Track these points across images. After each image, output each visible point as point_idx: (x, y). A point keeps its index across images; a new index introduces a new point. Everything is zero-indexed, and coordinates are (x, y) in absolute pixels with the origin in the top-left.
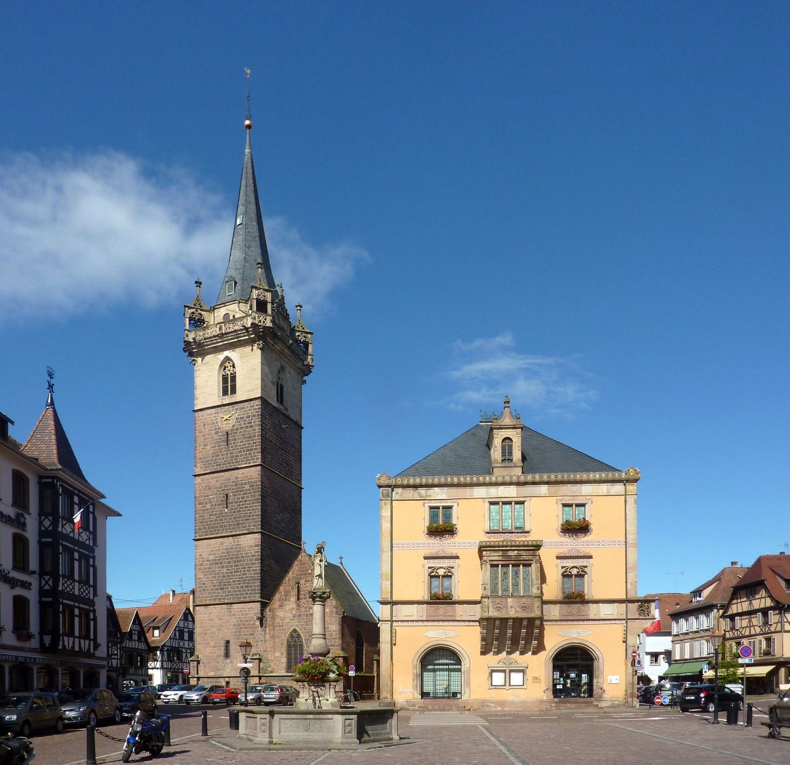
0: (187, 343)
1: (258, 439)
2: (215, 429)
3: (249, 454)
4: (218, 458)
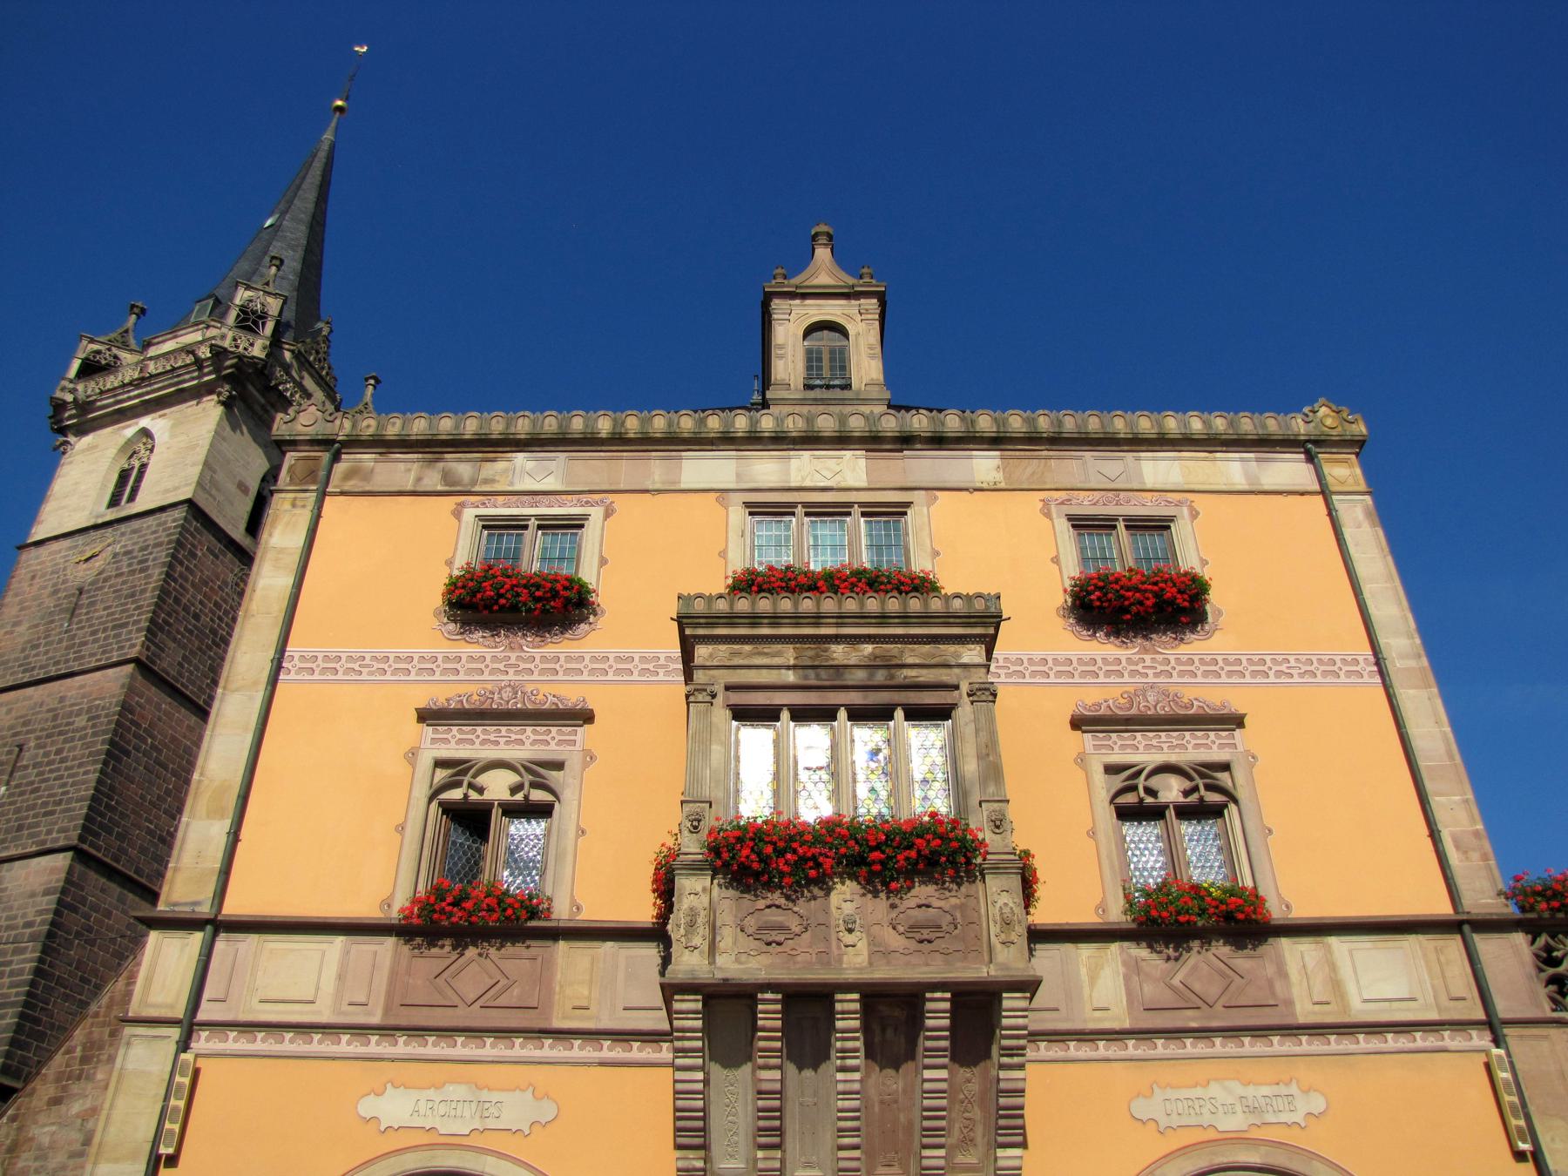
0: (60, 406)
1: (149, 599)
2: (54, 585)
3: (115, 636)
4: (34, 652)
